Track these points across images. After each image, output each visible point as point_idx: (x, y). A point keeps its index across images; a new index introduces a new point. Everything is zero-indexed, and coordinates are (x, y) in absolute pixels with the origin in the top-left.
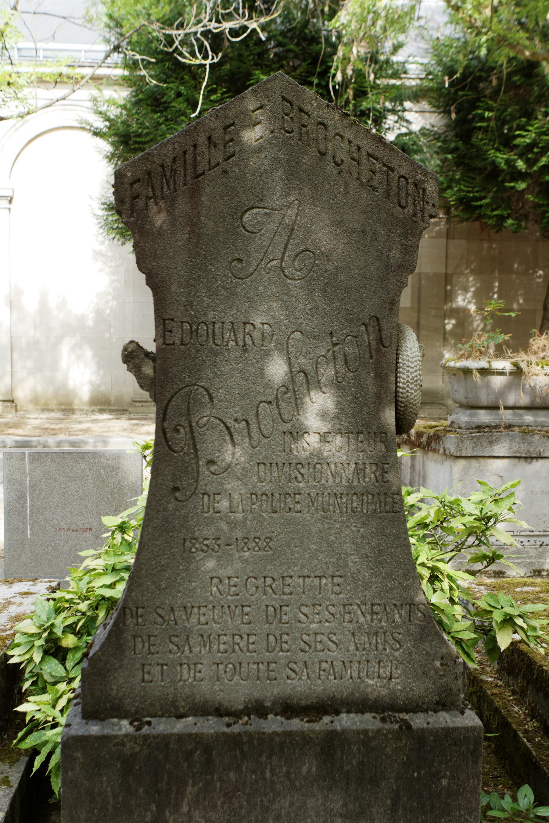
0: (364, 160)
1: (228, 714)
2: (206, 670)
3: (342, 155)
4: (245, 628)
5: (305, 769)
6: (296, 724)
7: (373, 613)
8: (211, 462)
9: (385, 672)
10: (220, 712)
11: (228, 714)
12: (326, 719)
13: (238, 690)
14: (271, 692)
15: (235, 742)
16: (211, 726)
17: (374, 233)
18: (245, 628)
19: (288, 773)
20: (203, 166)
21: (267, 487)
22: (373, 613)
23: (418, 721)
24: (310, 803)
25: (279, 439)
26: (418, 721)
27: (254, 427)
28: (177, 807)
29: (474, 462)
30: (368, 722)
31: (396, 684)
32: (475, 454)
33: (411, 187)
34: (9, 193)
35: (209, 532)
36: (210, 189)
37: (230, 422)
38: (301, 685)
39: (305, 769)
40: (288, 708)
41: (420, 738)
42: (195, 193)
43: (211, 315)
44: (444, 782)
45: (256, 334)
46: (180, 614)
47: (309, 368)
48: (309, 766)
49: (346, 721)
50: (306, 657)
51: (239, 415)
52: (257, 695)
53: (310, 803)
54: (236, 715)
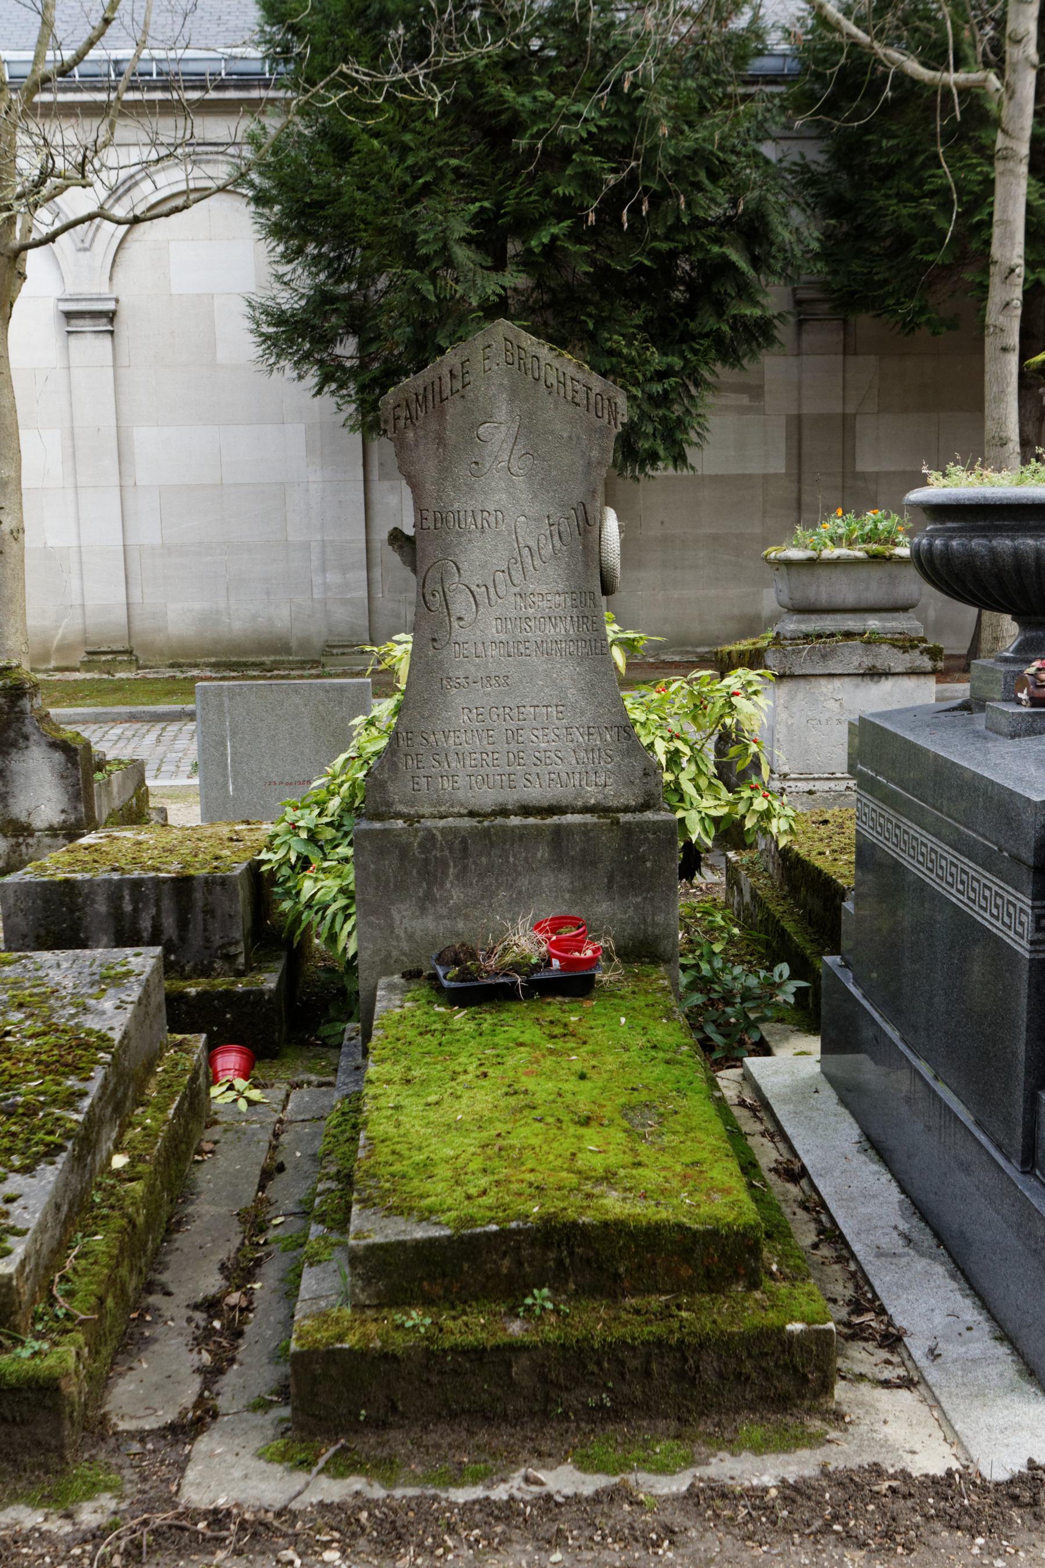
0: (569, 382)
1: (479, 815)
2: (462, 781)
3: (552, 380)
4: (490, 748)
5: (539, 855)
6: (531, 820)
7: (589, 734)
8: (460, 619)
9: (601, 781)
10: (471, 814)
11: (479, 815)
12: (555, 817)
13: (487, 798)
14: (512, 798)
15: (486, 833)
16: (467, 823)
17: (578, 438)
18: (490, 748)
19: (526, 859)
20: (447, 393)
21: (503, 637)
22: (589, 734)
23: (625, 818)
24: (544, 881)
25: (512, 599)
26: (625, 818)
27: (492, 590)
28: (442, 885)
29: (802, 684)
30: (589, 818)
31: (610, 791)
32: (804, 672)
33: (606, 402)
34: (110, 306)
35: (460, 673)
36: (453, 409)
37: (474, 588)
38: (536, 793)
39: (539, 855)
40: (526, 811)
41: (628, 830)
42: (442, 413)
43: (456, 505)
44: (648, 864)
45: (492, 520)
46: (440, 736)
47: (533, 544)
48: (543, 853)
49: (570, 818)
50: (538, 769)
51: (480, 582)
52: (500, 800)
53: (544, 881)
54: (486, 815)
